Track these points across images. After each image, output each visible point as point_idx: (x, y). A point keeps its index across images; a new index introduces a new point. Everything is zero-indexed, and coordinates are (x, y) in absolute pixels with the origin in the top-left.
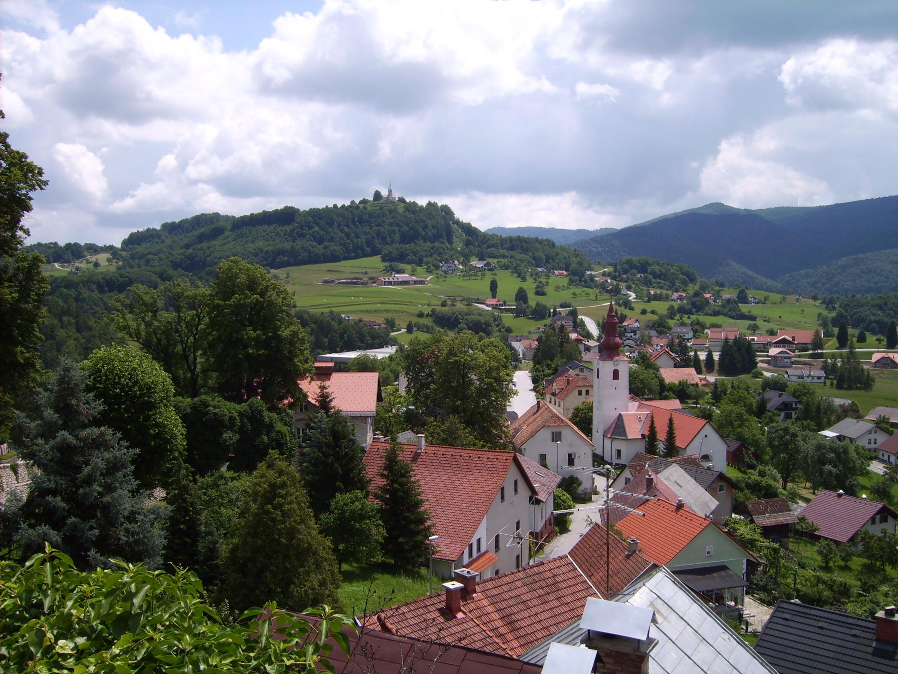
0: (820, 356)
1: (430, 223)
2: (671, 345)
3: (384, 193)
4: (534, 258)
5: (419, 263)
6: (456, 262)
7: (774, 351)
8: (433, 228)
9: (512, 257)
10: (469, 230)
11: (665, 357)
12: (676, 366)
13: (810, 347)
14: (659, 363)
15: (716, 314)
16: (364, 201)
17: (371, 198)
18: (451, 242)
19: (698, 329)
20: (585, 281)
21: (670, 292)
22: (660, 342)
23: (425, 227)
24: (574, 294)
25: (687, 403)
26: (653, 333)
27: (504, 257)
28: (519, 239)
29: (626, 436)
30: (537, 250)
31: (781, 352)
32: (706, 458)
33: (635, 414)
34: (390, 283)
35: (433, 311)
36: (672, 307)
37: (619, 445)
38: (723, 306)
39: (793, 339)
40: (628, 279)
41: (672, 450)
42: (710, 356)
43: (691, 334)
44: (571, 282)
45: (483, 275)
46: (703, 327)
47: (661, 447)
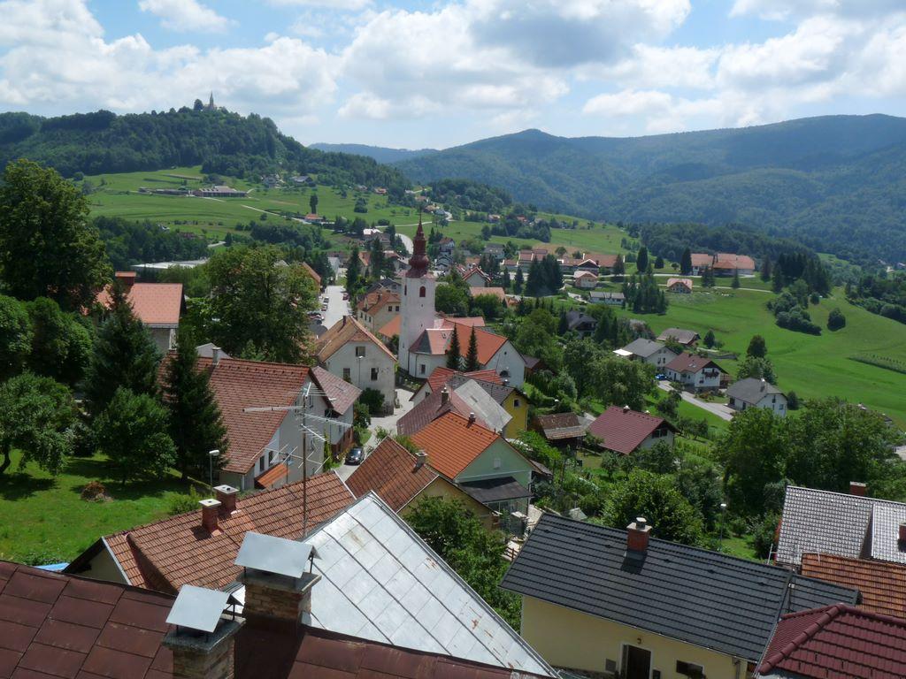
0: (620, 280)
1: (251, 135)
2: (482, 264)
3: (206, 102)
4: (355, 175)
5: (240, 176)
6: (277, 176)
7: (578, 274)
8: (255, 140)
9: (333, 173)
10: (292, 145)
11: (476, 277)
12: (486, 286)
13: (612, 271)
14: (469, 282)
15: (528, 236)
16: (184, 110)
17: (191, 106)
18: (273, 157)
19: (509, 252)
20: (405, 200)
21: (486, 214)
22: (473, 262)
23: (247, 139)
24: (394, 212)
25: (493, 321)
26: (467, 253)
27: (325, 172)
28: (341, 156)
29: (430, 351)
30: (359, 167)
31: (586, 275)
32: (504, 374)
33: (439, 330)
34: (209, 195)
35: (252, 224)
36: (486, 228)
37: (423, 360)
38: (535, 228)
39: (597, 262)
40: (446, 199)
41: (473, 365)
42: (519, 277)
43: (502, 255)
44: (391, 199)
45: (304, 190)
46: (515, 248)
47: (462, 362)
